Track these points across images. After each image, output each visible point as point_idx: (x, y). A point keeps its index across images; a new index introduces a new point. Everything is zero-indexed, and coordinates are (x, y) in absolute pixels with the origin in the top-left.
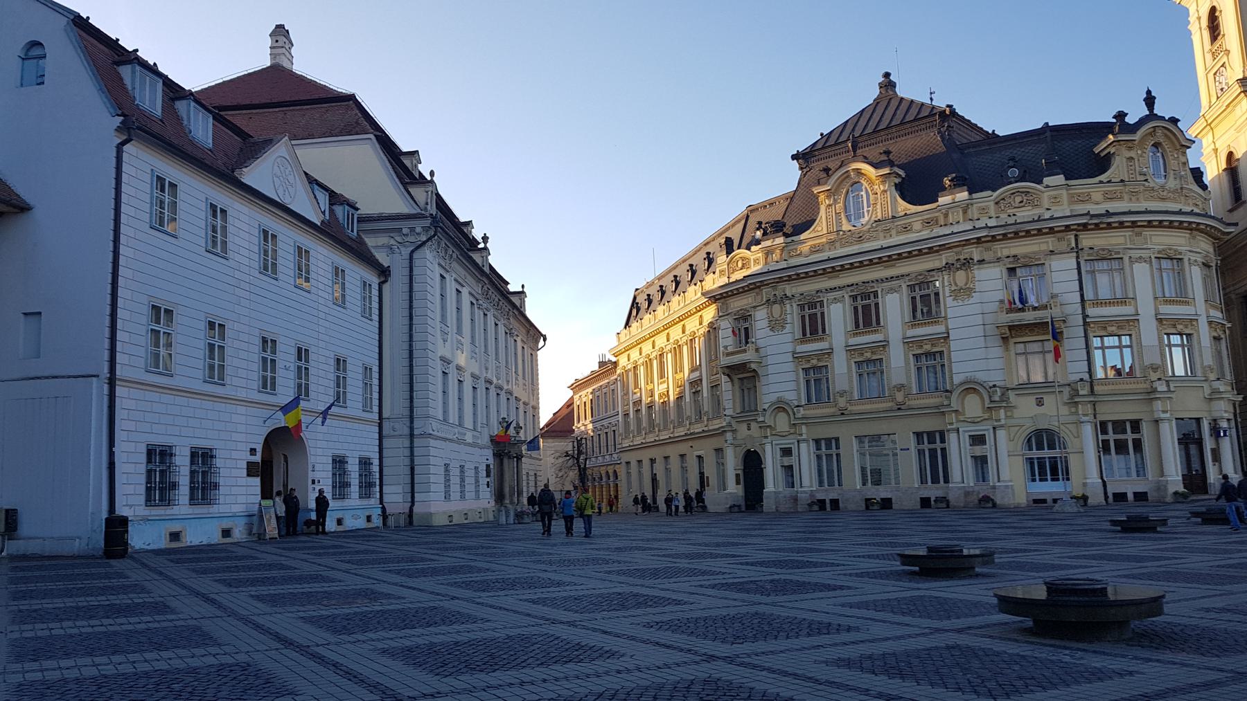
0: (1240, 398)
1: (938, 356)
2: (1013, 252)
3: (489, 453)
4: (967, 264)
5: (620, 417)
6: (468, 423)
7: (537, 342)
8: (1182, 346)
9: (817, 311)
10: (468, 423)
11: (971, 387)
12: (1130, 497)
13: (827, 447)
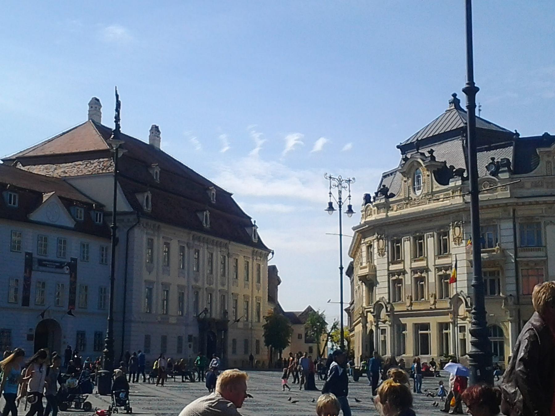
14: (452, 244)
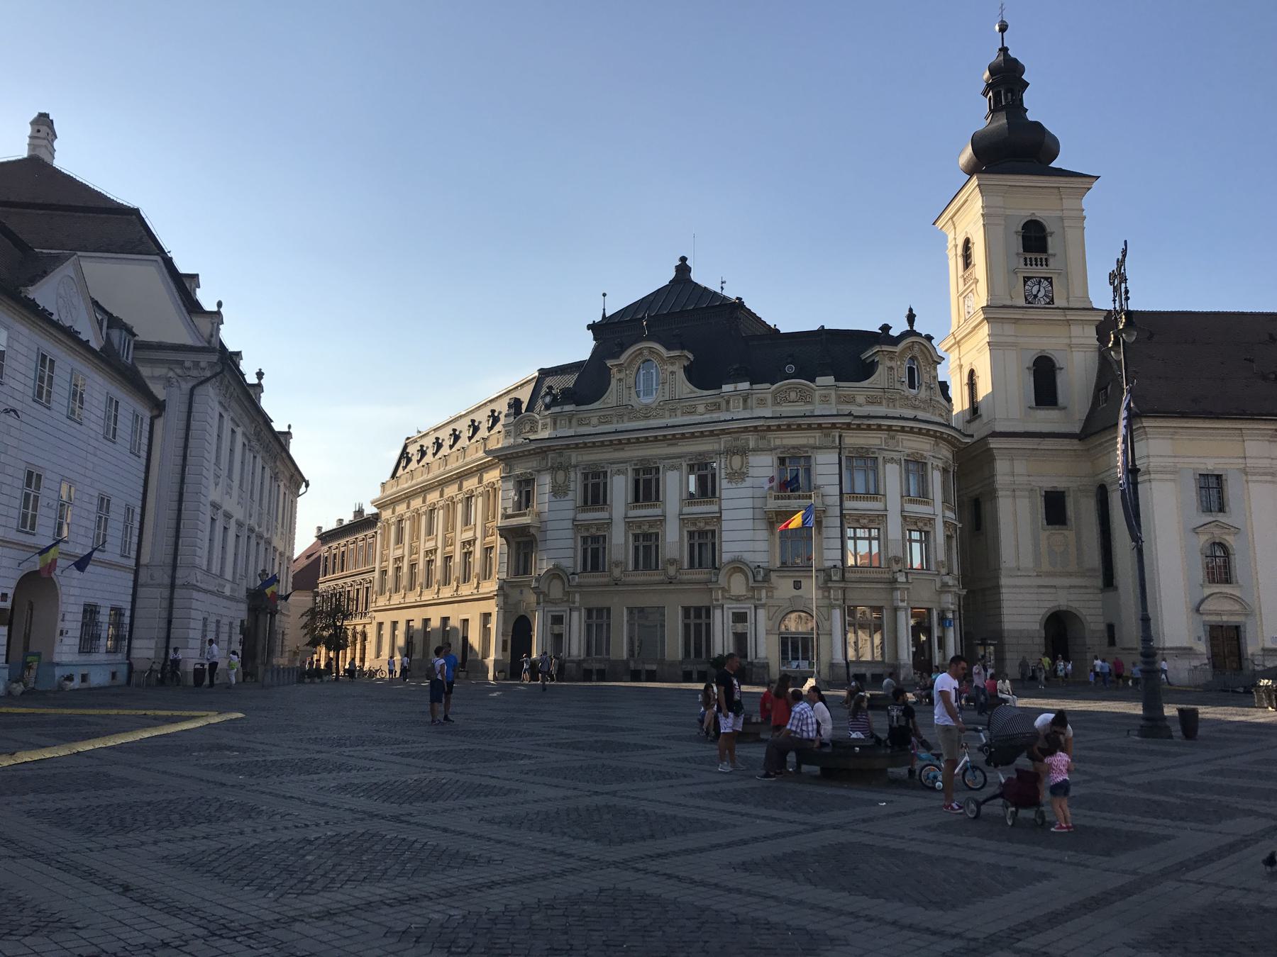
0: (964, 592)
1: (710, 535)
2: (786, 442)
3: (244, 607)
4: (743, 452)
5: (377, 574)
6: (228, 575)
7: (299, 488)
8: (920, 541)
9: (601, 481)
10: (228, 575)
11: (738, 566)
12: (868, 675)
13: (598, 618)
14: (725, 483)
